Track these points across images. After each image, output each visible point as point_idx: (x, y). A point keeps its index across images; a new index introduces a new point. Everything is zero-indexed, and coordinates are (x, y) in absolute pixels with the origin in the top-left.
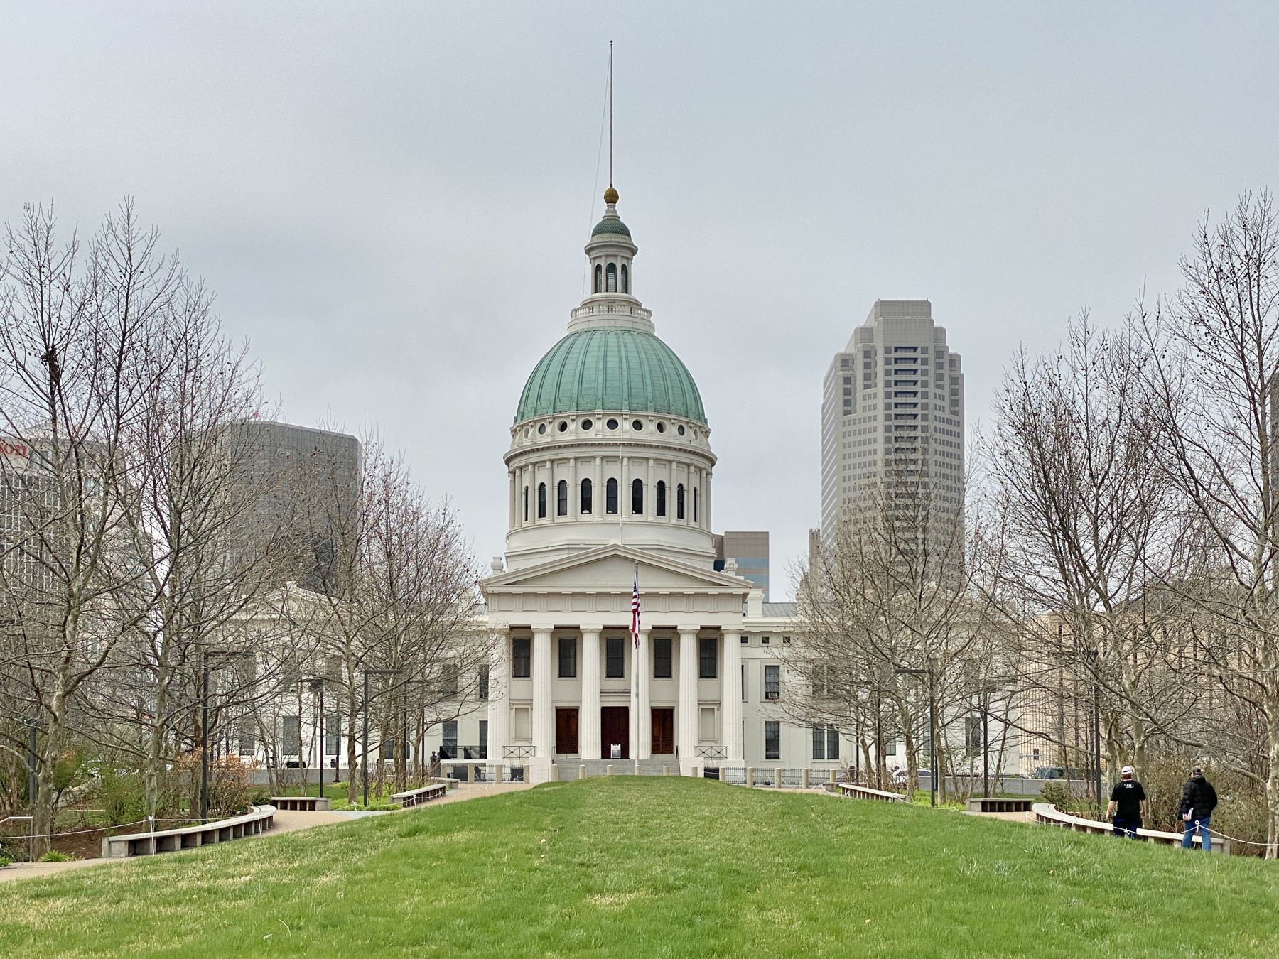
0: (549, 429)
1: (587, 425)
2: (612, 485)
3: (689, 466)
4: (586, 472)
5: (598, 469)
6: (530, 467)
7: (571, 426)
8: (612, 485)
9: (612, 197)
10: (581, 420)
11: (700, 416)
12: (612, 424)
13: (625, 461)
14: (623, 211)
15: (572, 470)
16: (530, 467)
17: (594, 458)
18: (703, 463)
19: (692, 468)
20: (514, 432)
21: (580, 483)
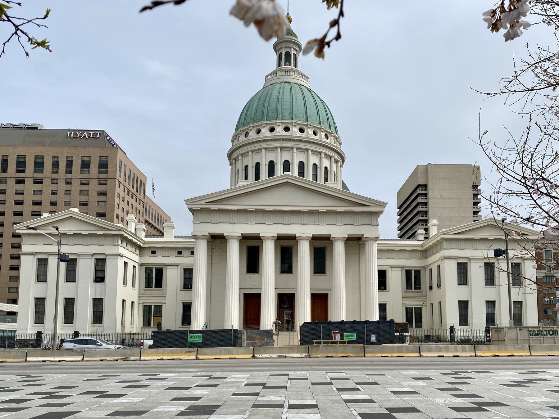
0: (250, 133)
1: (272, 130)
3: (331, 157)
4: (271, 156)
5: (279, 154)
6: (240, 157)
10: (268, 127)
11: (336, 132)
12: (287, 129)
13: (295, 150)
17: (276, 148)
18: (339, 159)
20: (233, 141)
21: (268, 163)
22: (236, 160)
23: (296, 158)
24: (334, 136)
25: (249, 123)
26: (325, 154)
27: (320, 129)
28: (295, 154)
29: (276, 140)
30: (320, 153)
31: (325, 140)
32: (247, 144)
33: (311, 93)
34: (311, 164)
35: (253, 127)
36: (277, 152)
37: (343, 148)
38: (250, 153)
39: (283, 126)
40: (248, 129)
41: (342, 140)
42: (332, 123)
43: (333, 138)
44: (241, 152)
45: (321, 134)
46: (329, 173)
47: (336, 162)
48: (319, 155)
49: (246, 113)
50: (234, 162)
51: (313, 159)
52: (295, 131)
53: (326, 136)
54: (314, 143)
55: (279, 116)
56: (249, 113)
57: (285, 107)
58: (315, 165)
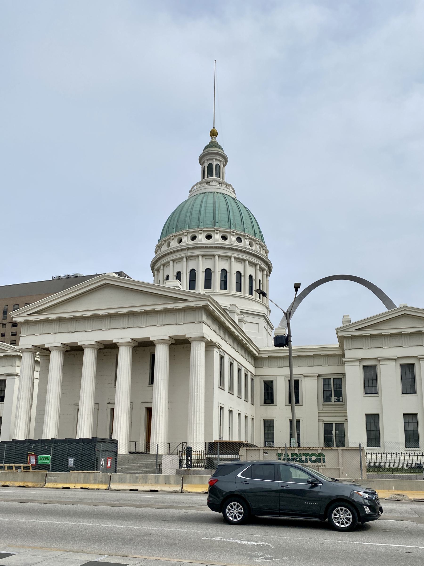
2: (208, 273)
3: (256, 265)
4: (192, 265)
5: (201, 262)
6: (162, 267)
7: (185, 239)
8: (208, 273)
9: (213, 134)
10: (190, 235)
11: (263, 240)
13: (217, 258)
14: (218, 139)
15: (185, 264)
16: (162, 267)
17: (197, 256)
19: (258, 267)
21: (189, 271)
22: (158, 270)
23: (219, 266)
24: (260, 244)
25: (171, 233)
26: (249, 262)
27: (244, 236)
28: (217, 262)
29: (198, 248)
30: (244, 261)
31: (249, 247)
32: (168, 254)
33: (235, 201)
34: (234, 272)
35: (175, 236)
36: (199, 260)
37: (271, 258)
38: (171, 263)
39: (205, 234)
40: (169, 239)
41: (268, 248)
42: (257, 231)
43: (258, 246)
44: (163, 263)
45: (245, 241)
46: (254, 282)
47: (262, 270)
48: (243, 263)
49: (170, 223)
50: (156, 273)
51: (237, 267)
52: (217, 238)
53: (251, 244)
54: (237, 250)
55: (201, 224)
56: (171, 223)
57: (207, 215)
58: (238, 273)
